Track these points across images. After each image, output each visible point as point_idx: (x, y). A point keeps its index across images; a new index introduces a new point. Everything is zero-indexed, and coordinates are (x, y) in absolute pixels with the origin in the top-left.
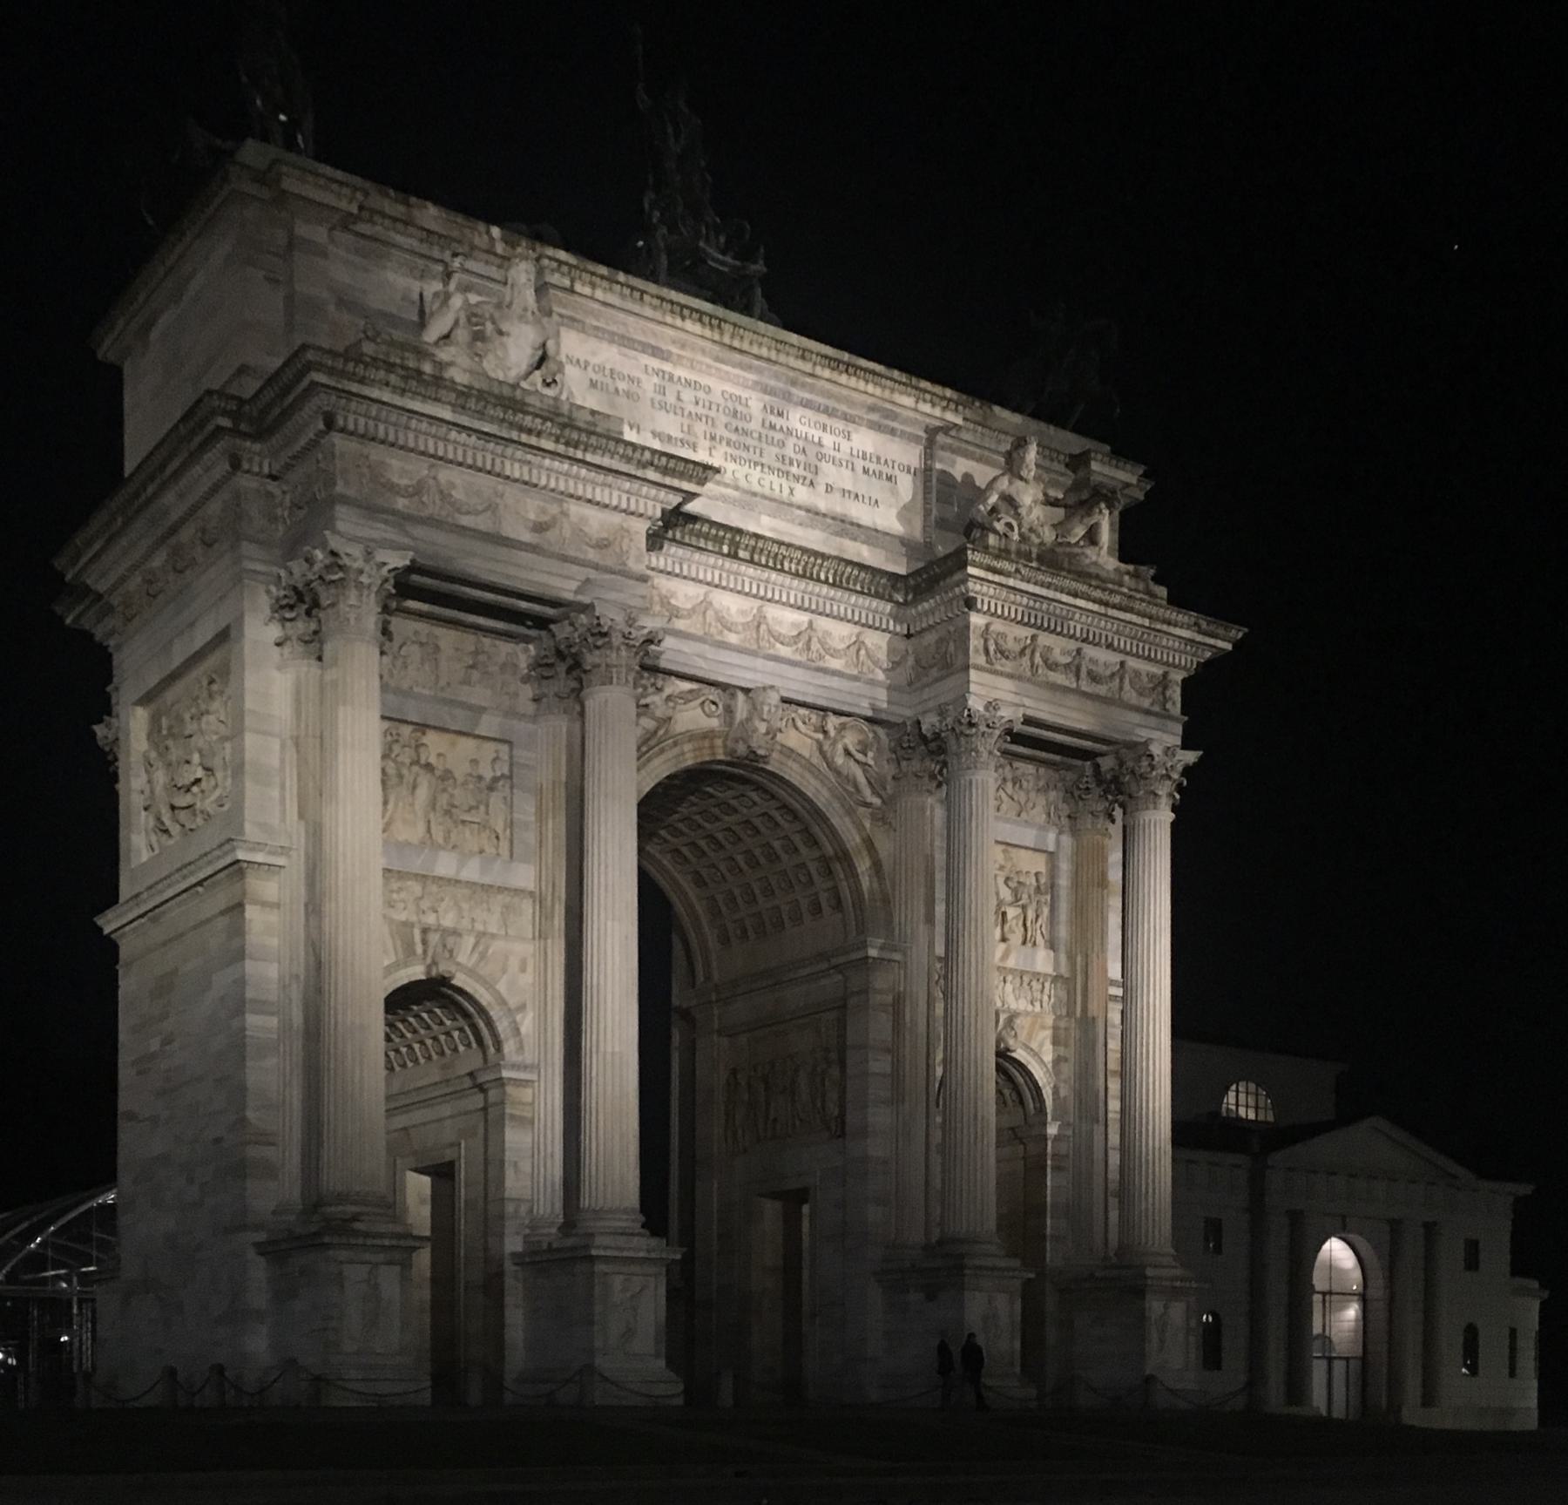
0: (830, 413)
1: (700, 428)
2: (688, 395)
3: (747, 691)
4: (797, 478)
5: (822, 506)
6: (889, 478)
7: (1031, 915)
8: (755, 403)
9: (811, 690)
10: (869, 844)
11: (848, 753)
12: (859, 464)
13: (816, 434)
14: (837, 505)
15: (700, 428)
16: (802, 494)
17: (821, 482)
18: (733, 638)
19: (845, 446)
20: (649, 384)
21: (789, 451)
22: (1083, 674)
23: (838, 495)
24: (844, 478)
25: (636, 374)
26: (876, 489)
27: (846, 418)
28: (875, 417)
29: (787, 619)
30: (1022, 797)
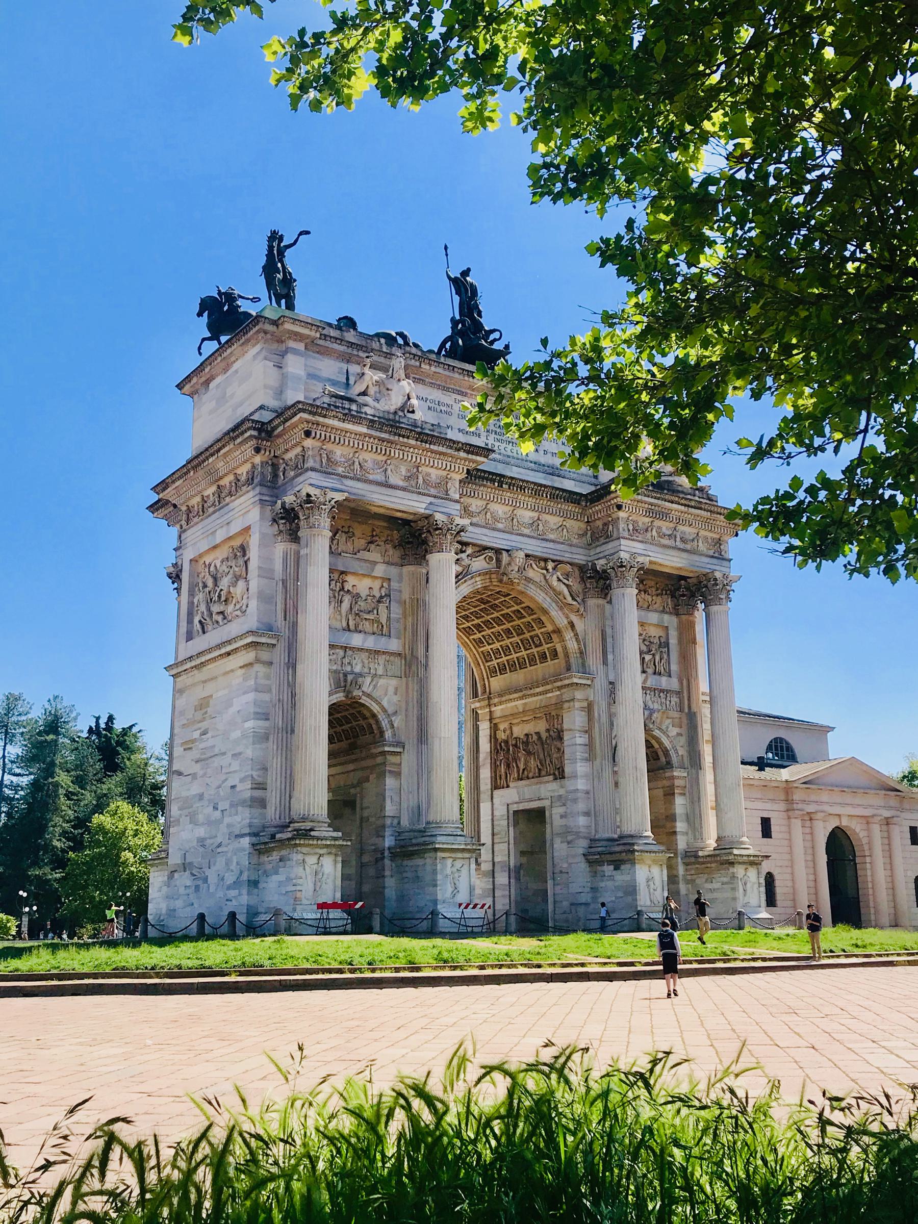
3: (508, 551)
7: (657, 658)
9: (540, 549)
10: (572, 625)
11: (559, 580)
18: (500, 526)
22: (678, 539)
23: (549, 455)
25: (450, 403)
29: (526, 515)
30: (649, 598)
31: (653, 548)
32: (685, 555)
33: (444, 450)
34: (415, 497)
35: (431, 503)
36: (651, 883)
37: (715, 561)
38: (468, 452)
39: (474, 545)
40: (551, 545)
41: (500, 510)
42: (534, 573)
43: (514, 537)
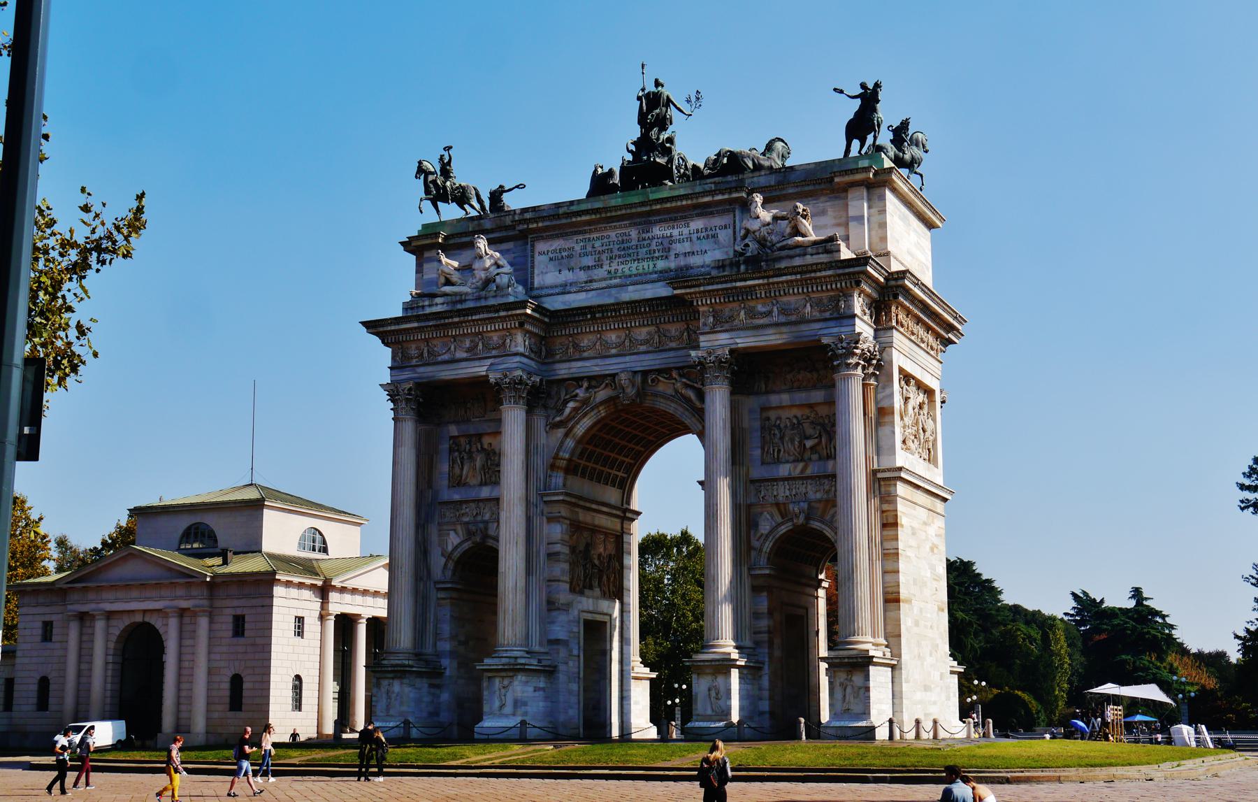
0: (675, 219)
1: (604, 257)
2: (597, 244)
4: (657, 258)
5: (673, 265)
6: (713, 236)
8: (634, 233)
12: (694, 237)
13: (668, 232)
14: (682, 262)
15: (604, 257)
16: (661, 265)
17: (672, 253)
18: (614, 351)
19: (685, 231)
20: (578, 248)
21: (654, 247)
23: (682, 257)
24: (687, 247)
26: (705, 245)
27: (683, 218)
28: (698, 211)
30: (815, 375)
31: (742, 333)
32: (784, 329)
33: (486, 316)
34: (477, 363)
35: (492, 364)
36: (713, 694)
37: (831, 324)
38: (507, 310)
39: (590, 378)
40: (672, 354)
41: (613, 337)
42: (664, 387)
43: (627, 358)
